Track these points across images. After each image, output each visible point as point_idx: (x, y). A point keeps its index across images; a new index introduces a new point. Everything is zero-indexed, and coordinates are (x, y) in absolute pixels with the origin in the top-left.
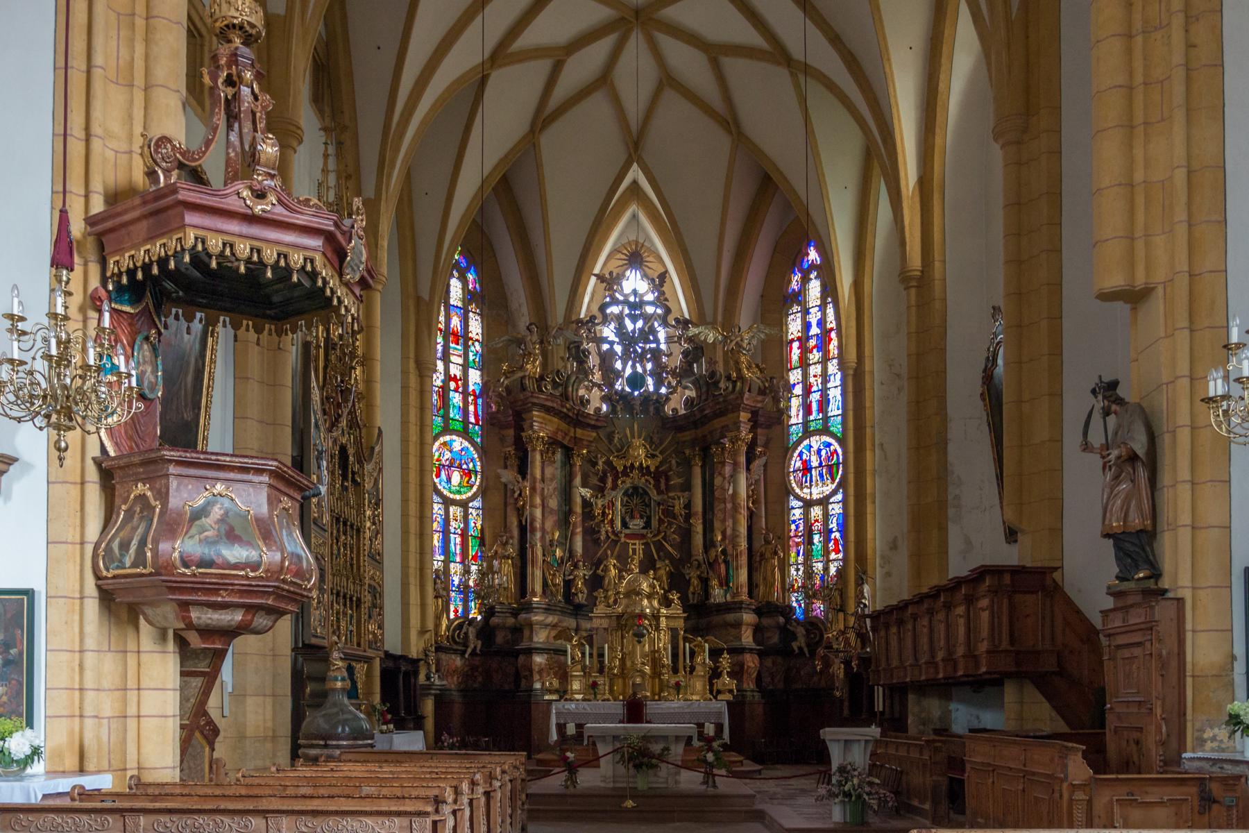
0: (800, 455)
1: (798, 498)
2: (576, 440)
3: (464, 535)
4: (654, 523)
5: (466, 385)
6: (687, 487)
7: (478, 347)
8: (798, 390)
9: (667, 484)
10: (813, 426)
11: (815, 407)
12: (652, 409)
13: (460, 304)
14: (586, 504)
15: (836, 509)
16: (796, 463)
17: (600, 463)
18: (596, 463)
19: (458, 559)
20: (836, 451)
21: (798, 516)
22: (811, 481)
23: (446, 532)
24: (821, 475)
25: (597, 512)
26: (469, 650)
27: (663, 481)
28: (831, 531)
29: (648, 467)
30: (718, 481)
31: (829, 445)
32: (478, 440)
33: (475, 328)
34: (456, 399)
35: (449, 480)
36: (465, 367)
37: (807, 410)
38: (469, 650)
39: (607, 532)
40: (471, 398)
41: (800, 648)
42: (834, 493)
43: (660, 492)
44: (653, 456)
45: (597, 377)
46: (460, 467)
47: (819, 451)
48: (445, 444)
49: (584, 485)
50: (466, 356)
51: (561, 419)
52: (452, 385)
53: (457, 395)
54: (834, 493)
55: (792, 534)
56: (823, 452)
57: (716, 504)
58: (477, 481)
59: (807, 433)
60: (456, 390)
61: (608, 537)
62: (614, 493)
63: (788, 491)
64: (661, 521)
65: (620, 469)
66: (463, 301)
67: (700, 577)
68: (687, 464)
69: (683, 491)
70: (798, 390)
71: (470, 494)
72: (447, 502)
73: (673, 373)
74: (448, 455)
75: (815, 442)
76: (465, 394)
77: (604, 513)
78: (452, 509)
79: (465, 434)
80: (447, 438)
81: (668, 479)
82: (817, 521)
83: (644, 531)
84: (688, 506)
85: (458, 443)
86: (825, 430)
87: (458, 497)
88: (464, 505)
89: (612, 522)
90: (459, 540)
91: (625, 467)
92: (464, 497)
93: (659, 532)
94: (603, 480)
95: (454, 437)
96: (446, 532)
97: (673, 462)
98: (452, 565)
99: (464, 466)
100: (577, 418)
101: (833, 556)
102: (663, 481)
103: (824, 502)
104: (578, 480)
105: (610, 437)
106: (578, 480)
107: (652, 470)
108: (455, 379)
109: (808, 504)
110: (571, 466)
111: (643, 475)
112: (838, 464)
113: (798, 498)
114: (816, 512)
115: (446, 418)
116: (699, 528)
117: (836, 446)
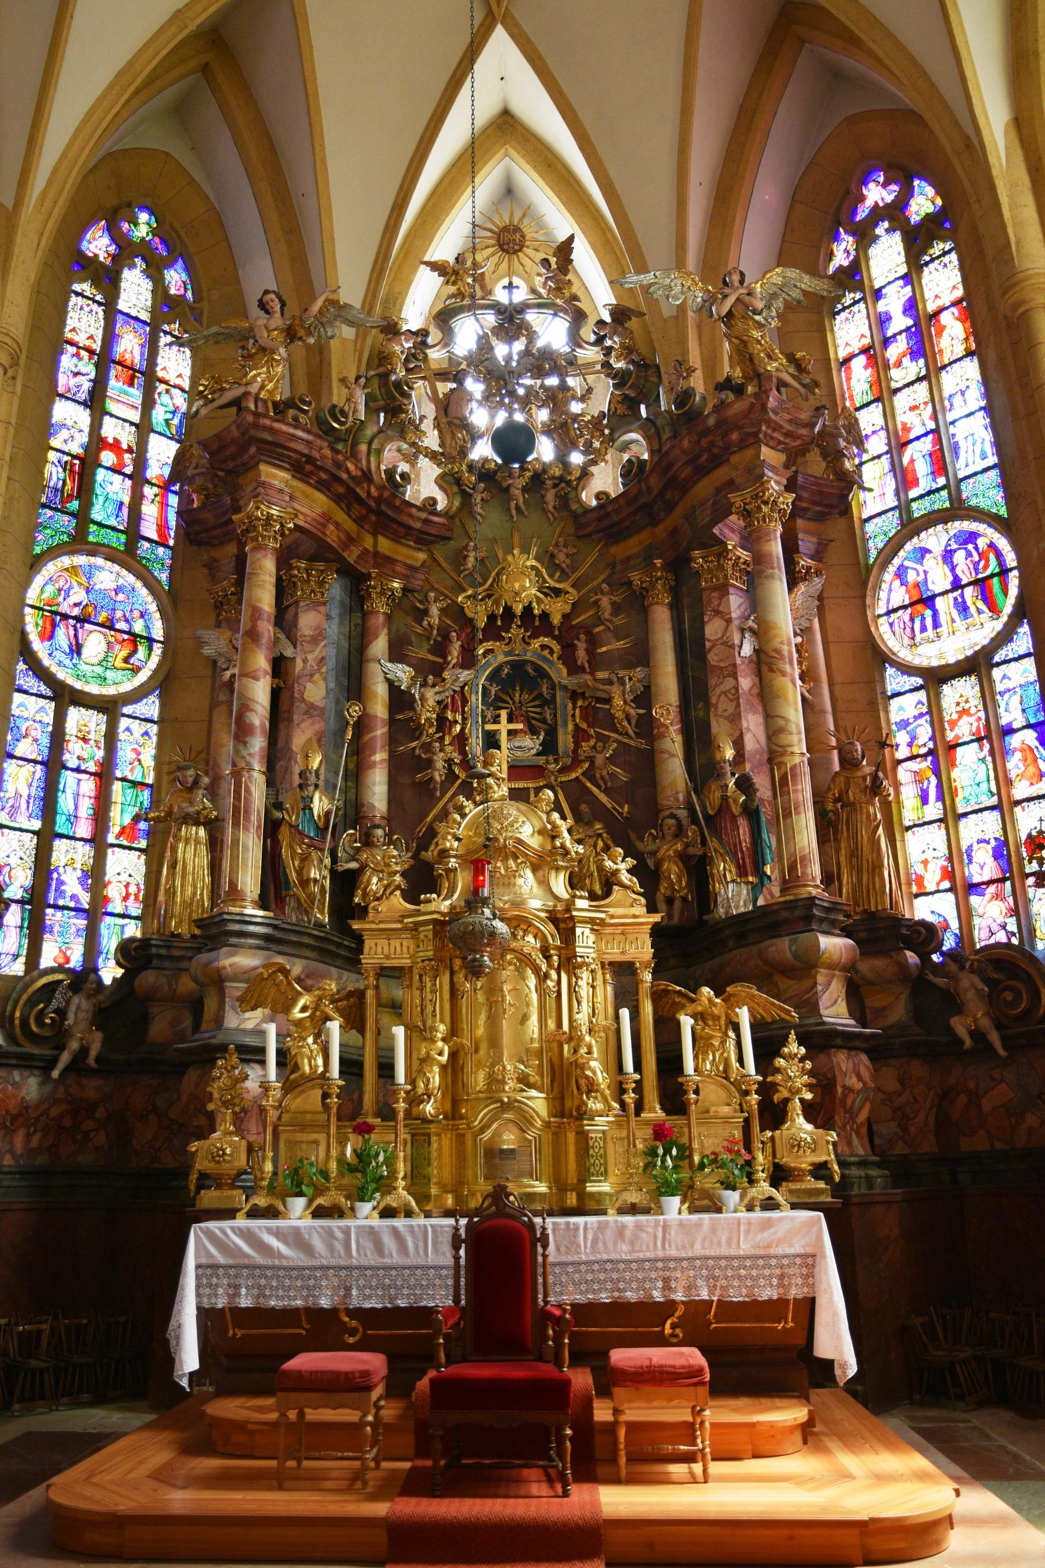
0: (901, 574)
1: (907, 669)
2: (385, 562)
3: (104, 775)
4: (565, 740)
5: (141, 463)
6: (641, 655)
7: (180, 400)
8: (877, 444)
9: (591, 653)
10: (919, 509)
11: (922, 468)
12: (550, 496)
13: (145, 316)
14: (400, 699)
15: (1017, 675)
16: (891, 593)
17: (434, 611)
18: (426, 612)
19: (84, 829)
20: (992, 546)
21: (910, 712)
22: (936, 625)
23: (53, 765)
24: (963, 608)
25: (427, 714)
26: (65, 1058)
27: (581, 647)
28: (1009, 731)
29: (545, 616)
30: (713, 629)
31: (972, 537)
32: (164, 577)
33: (175, 364)
34: (111, 488)
35: (76, 649)
36: (144, 428)
37: (905, 479)
38: (65, 1058)
39: (449, 762)
40: (149, 491)
41: (977, 1035)
42: (1005, 637)
43: (574, 669)
44: (557, 592)
45: (431, 440)
46: (109, 625)
47: (948, 556)
48: (73, 570)
49: (396, 654)
50: (148, 404)
51: (337, 499)
52: (108, 458)
53: (117, 479)
54: (1005, 637)
55: (902, 753)
56: (959, 557)
57: (713, 681)
58: (150, 661)
59: (911, 527)
60: (116, 470)
61: (451, 776)
62: (465, 675)
63: (881, 657)
64: (579, 735)
65: (482, 622)
66: (154, 311)
67: (683, 857)
68: (637, 604)
69: (631, 666)
70: (877, 444)
71: (127, 687)
72: (64, 697)
73: (596, 423)
74: (78, 595)
75: (935, 539)
76: (138, 478)
77: (442, 720)
78: (75, 717)
79: (127, 556)
80: (82, 560)
81: (593, 642)
82: (965, 712)
83: (541, 760)
84: (645, 698)
85: (108, 576)
86: (959, 509)
87: (94, 689)
88: (109, 708)
89: (461, 740)
90: (89, 786)
91: (492, 618)
92: (112, 691)
93: (576, 762)
94: (441, 649)
95: (99, 561)
96: (53, 765)
97: (605, 601)
98: (60, 847)
99: (121, 625)
100: (381, 507)
101: (1020, 791)
102: (581, 647)
103: (978, 665)
104: (380, 646)
105: (458, 559)
106: (380, 646)
107: (556, 620)
108: (115, 446)
109: (935, 679)
110: (365, 615)
111: (535, 636)
112: (1004, 572)
113: (907, 669)
114: (960, 693)
115: (83, 517)
116: (673, 743)
117: (988, 534)
